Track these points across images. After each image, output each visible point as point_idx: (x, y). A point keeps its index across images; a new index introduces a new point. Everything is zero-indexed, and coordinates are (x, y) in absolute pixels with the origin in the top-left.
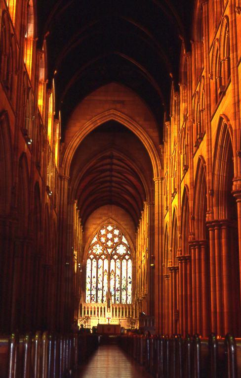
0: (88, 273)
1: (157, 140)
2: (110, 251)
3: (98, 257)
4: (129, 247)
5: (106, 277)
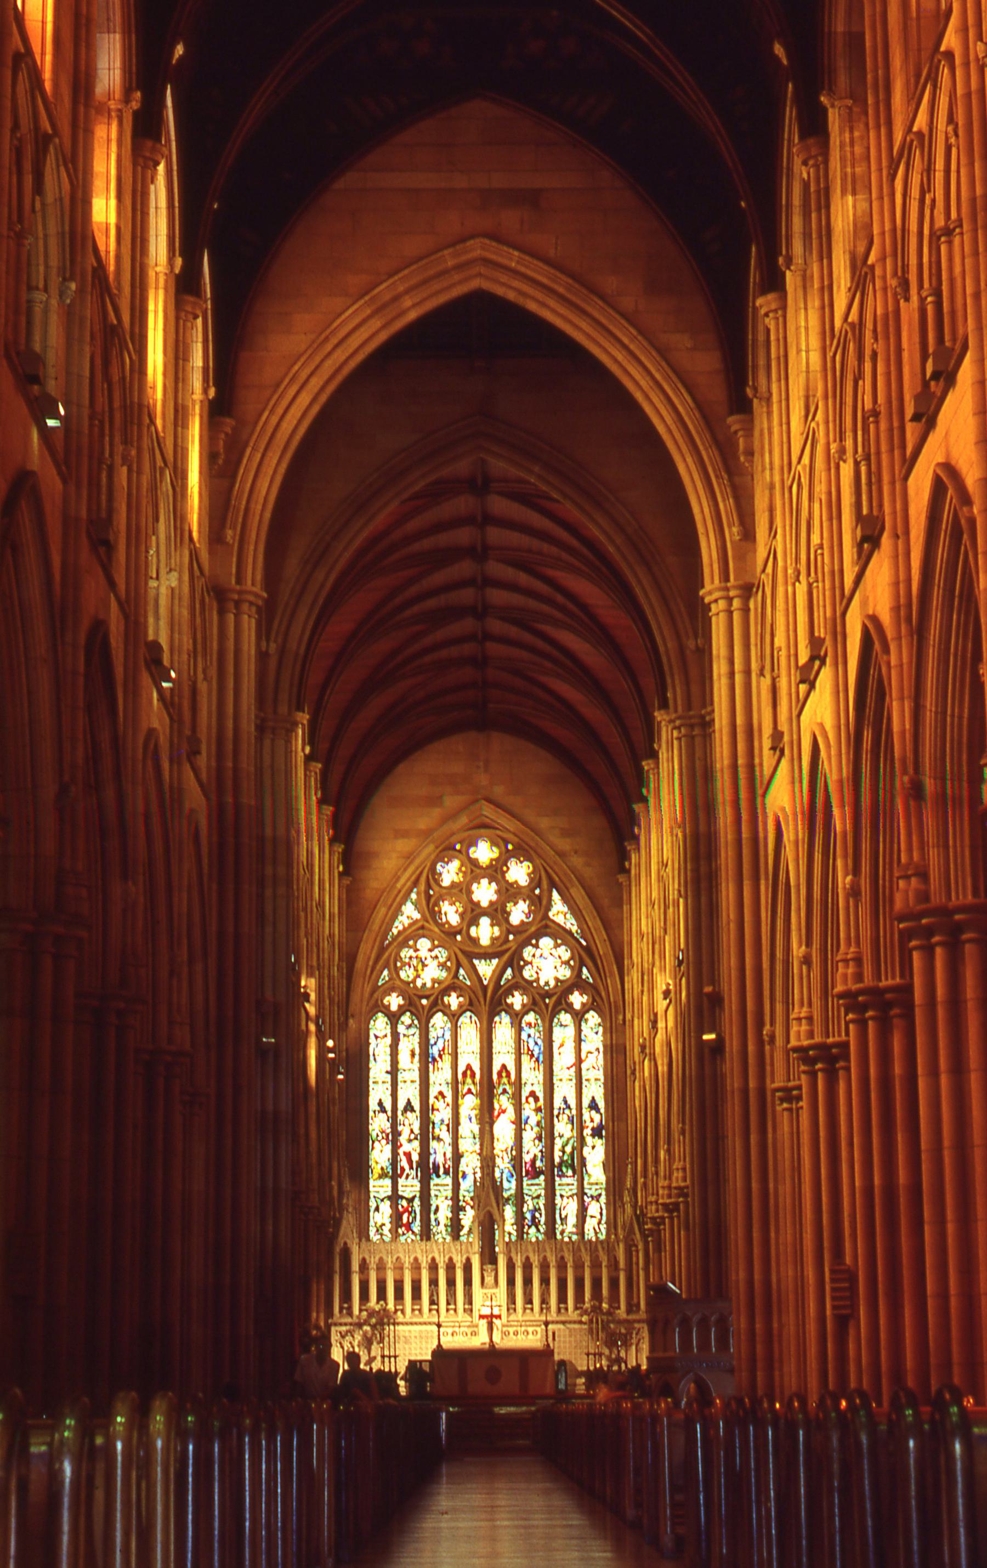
0: (378, 1092)
1: (717, 393)
2: (486, 969)
3: (424, 1002)
4: (587, 949)
5: (469, 1105)
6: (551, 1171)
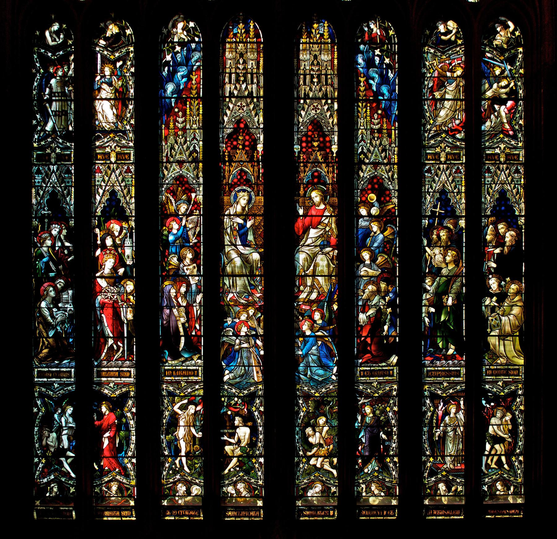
6: (413, 344)
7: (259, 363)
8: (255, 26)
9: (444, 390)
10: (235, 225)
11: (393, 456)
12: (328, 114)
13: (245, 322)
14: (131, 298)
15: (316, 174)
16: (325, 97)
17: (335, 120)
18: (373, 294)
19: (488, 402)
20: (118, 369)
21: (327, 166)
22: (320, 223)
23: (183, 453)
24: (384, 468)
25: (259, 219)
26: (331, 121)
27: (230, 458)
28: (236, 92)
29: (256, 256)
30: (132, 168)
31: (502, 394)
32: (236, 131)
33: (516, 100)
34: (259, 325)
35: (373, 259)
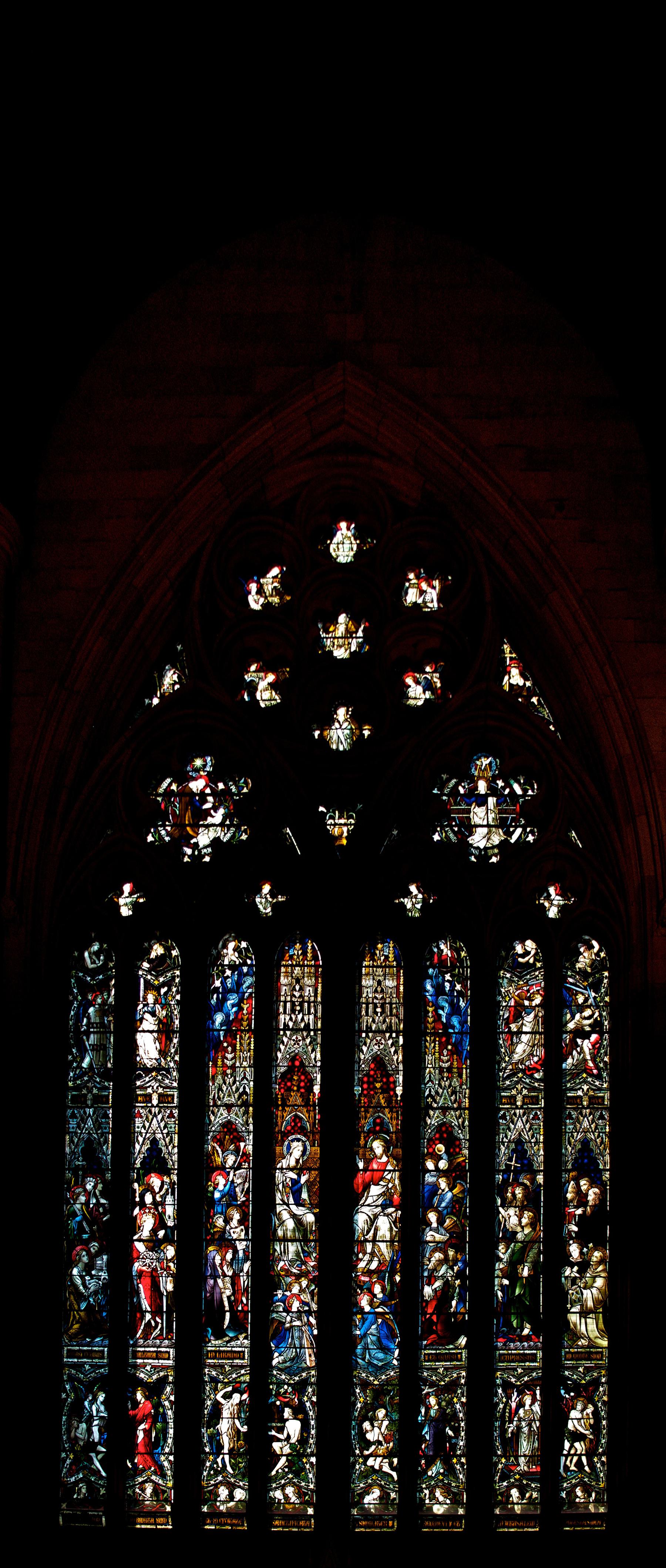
6: (484, 1323)
7: (312, 1344)
8: (313, 947)
9: (519, 1377)
10: (288, 1180)
11: (461, 1456)
12: (393, 1050)
13: (297, 1296)
14: (171, 1265)
15: (378, 1121)
16: (389, 1029)
17: (401, 1058)
18: (440, 1263)
19: (568, 1392)
20: (155, 1349)
21: (391, 1111)
22: (382, 1178)
23: (226, 1450)
24: (450, 1470)
25: (314, 1173)
26: (395, 1058)
27: (278, 1457)
28: (291, 1024)
29: (310, 1218)
30: (176, 1112)
31: (583, 1382)
32: (291, 1069)
33: (601, 1034)
34: (312, 1299)
35: (441, 1221)
